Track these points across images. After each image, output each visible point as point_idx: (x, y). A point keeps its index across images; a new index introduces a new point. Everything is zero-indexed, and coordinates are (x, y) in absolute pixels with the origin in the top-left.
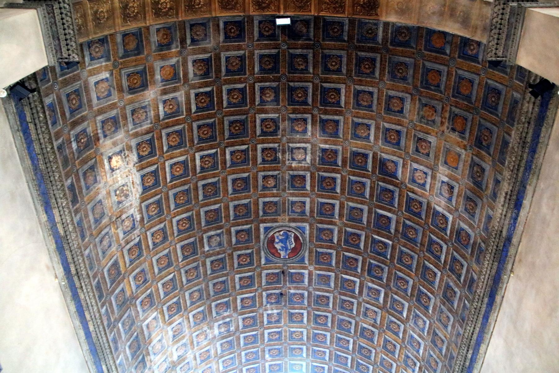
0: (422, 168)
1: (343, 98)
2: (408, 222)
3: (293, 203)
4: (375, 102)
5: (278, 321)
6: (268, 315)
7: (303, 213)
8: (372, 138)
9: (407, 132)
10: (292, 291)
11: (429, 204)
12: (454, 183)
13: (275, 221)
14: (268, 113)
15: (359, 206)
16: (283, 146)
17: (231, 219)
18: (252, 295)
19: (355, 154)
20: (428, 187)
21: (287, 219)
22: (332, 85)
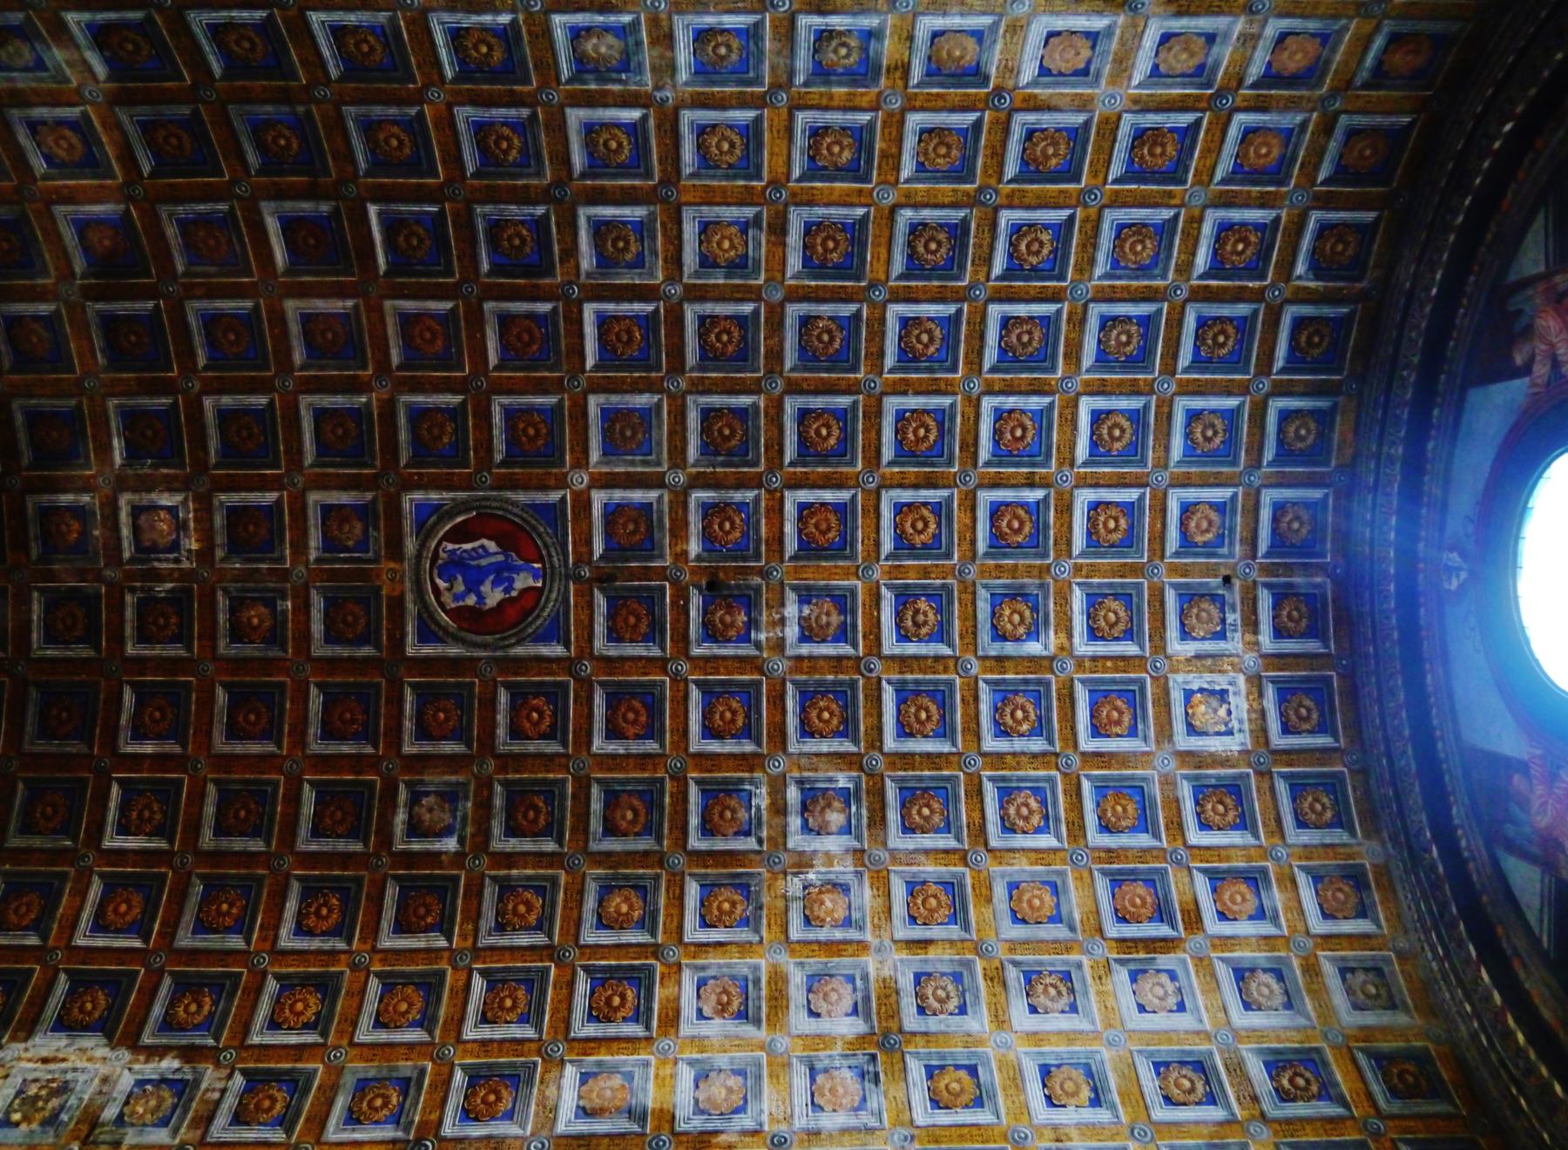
3: (330, 544)
5: (843, 601)
6: (804, 638)
7: (364, 513)
10: (694, 547)
13: (397, 604)
14: (30, 621)
16: (130, 576)
17: (369, 750)
18: (695, 694)
19: (118, 356)
21: (392, 565)
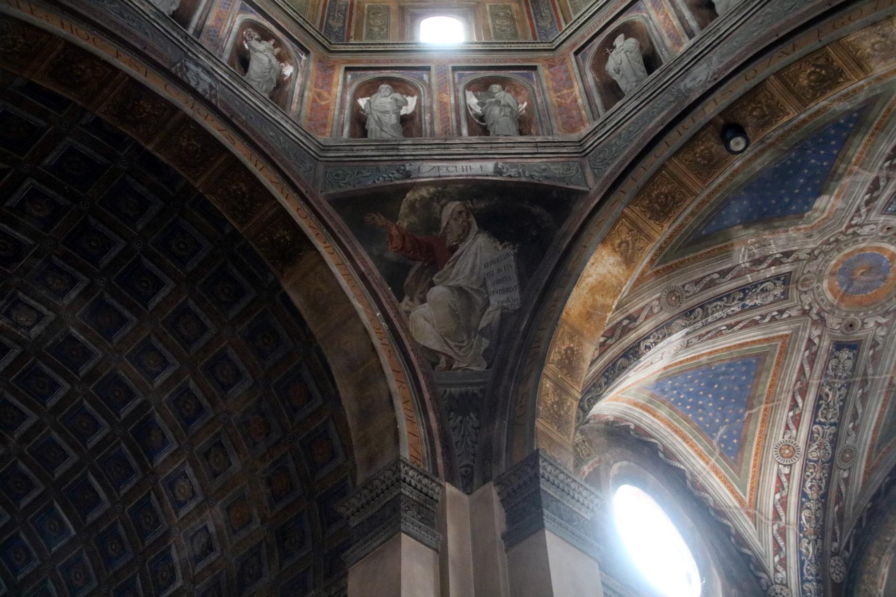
0: (195, 481)
1: (158, 299)
2: (121, 528)
4: (202, 342)
8: (159, 381)
9: (212, 419)
11: (167, 535)
12: (217, 546)
15: (66, 447)
20: (183, 512)
22: (157, 272)
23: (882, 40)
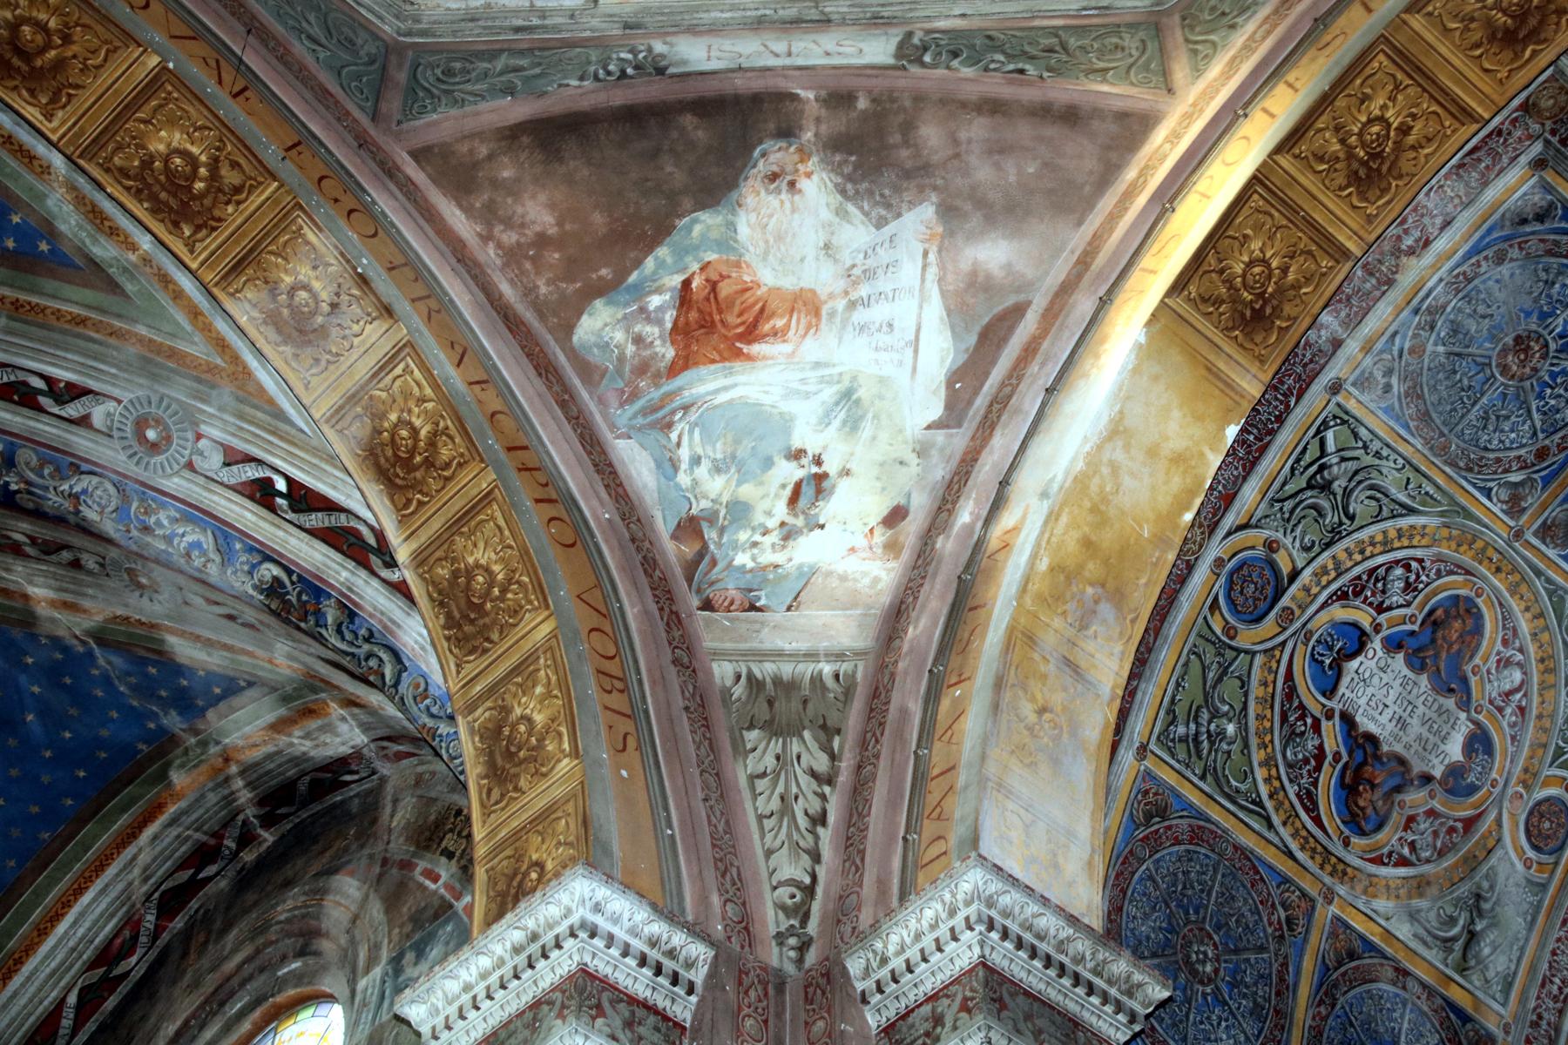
23: (325, 307)
